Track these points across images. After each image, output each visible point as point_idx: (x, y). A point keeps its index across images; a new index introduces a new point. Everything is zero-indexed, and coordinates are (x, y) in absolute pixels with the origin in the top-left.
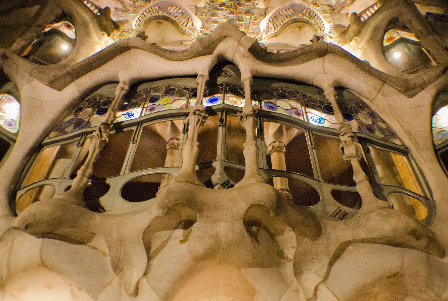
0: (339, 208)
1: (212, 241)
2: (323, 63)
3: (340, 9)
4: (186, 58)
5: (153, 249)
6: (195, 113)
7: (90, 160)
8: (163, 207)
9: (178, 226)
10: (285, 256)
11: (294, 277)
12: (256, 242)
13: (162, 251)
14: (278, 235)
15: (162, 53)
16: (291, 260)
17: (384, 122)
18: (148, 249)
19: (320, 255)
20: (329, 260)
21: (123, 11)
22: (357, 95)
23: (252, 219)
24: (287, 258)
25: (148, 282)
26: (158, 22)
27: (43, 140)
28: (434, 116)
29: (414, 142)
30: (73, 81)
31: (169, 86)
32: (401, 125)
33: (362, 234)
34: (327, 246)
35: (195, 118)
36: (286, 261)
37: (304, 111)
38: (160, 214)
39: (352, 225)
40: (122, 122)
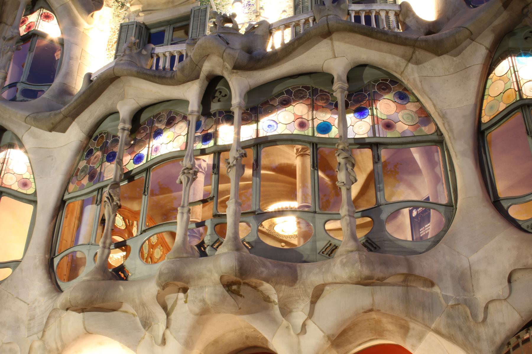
0: (330, 241)
2: (332, 44)
5: (169, 307)
6: (184, 173)
12: (239, 297)
14: (260, 286)
17: (418, 100)
18: (165, 307)
20: (310, 300)
24: (274, 302)
25: (171, 333)
27: (63, 196)
28: (491, 75)
29: (447, 128)
30: (74, 120)
32: (435, 106)
35: (185, 178)
36: (273, 304)
37: (310, 118)
39: (323, 270)
40: (132, 171)
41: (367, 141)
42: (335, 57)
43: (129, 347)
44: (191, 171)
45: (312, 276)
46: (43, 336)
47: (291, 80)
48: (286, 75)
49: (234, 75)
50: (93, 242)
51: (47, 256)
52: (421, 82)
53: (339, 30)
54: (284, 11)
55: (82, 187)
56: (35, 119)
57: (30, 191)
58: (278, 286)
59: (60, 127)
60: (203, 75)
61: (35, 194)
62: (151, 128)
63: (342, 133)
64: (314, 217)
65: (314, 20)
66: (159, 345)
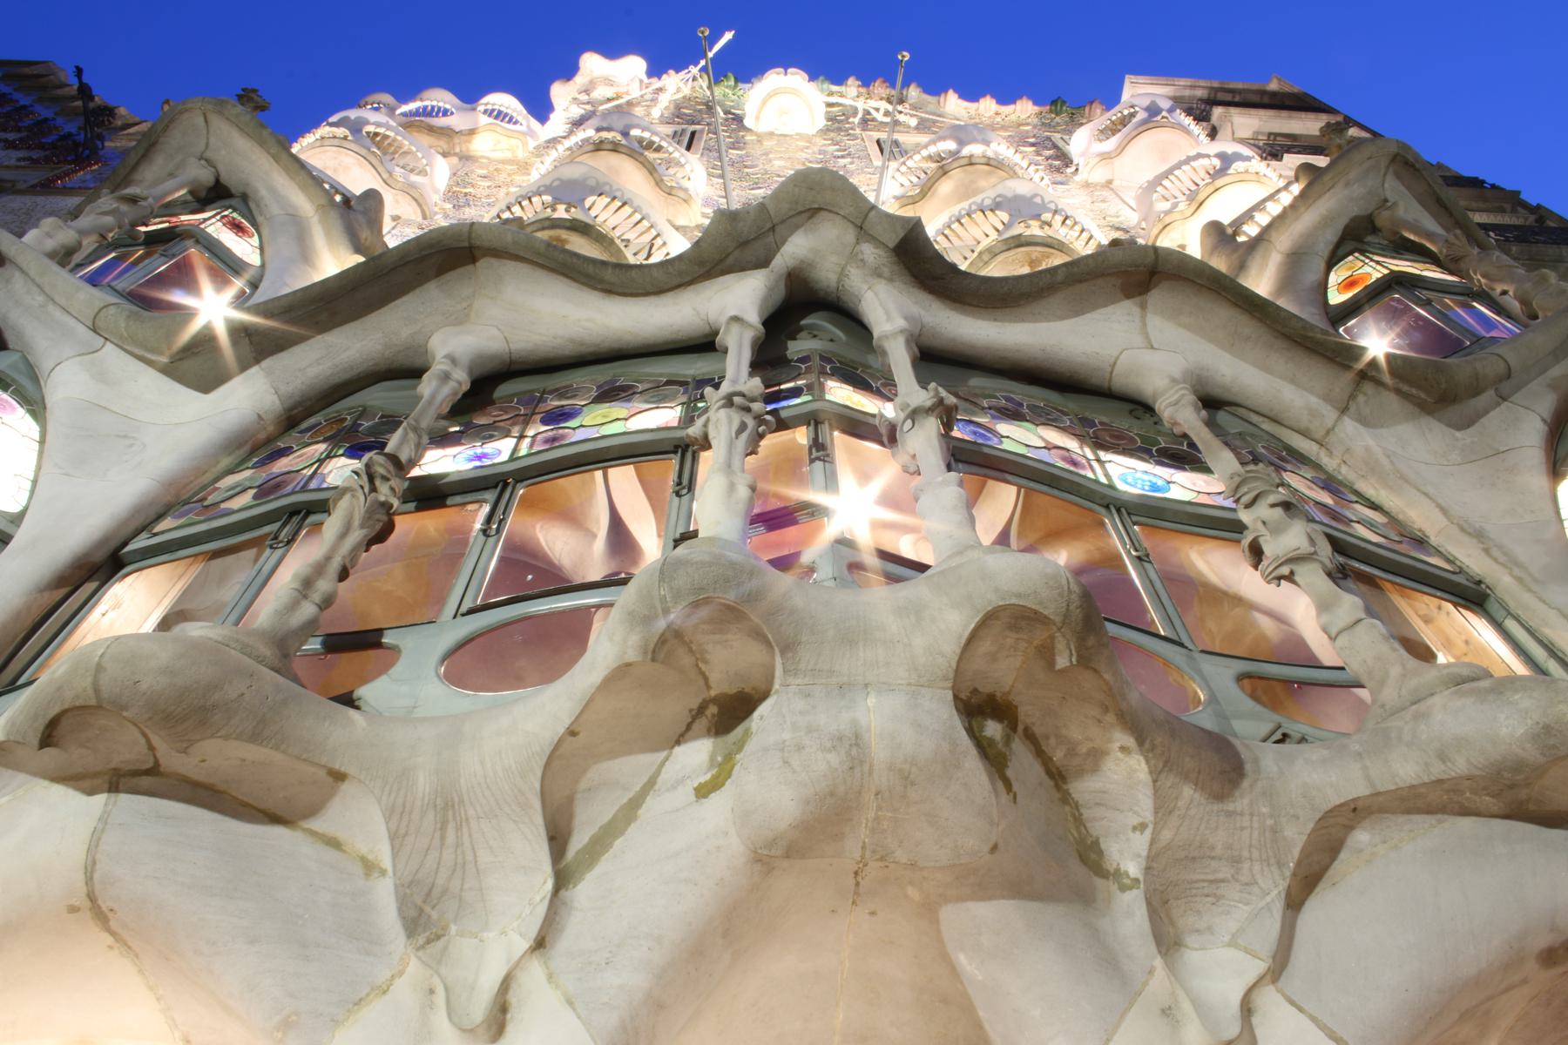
0: (1279, 727)
1: (834, 759)
2: (1143, 318)
3: (1155, 231)
4: (677, 281)
5: (578, 841)
9: (689, 727)
11: (1153, 948)
12: (1000, 784)
13: (618, 843)
14: (1081, 772)
15: (591, 269)
16: (1137, 880)
17: (1375, 507)
18: (557, 839)
19: (1246, 865)
20: (1283, 885)
22: (1267, 426)
23: (986, 688)
24: (1117, 875)
27: (125, 544)
29: (1502, 559)
30: (257, 361)
32: (1444, 511)
33: (1405, 769)
34: (1270, 822)
38: (632, 656)
58: (1168, 780)
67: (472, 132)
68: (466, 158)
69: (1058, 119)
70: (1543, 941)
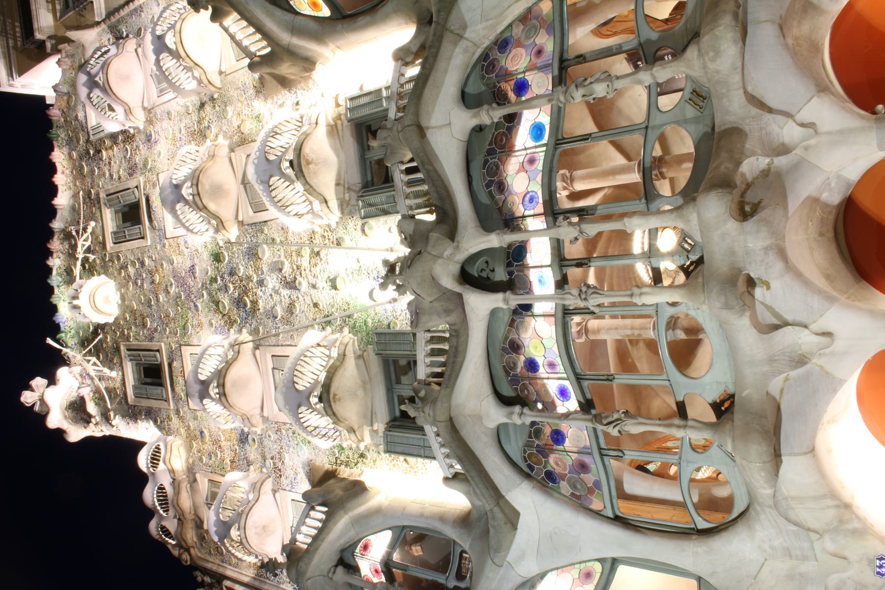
1: (771, 254)
3: (212, 88)
7: (660, 425)
8: (744, 311)
10: (767, 167)
12: (761, 205)
14: (746, 179)
17: (510, 25)
18: (776, 327)
20: (767, 114)
21: (281, 476)
22: (469, 70)
24: (769, 164)
26: (335, 402)
27: (608, 518)
30: (503, 497)
31: (503, 349)
33: (737, 78)
37: (524, 152)
39: (724, 91)
40: (579, 402)
41: (556, 72)
42: (450, 124)
43: (835, 391)
44: (584, 289)
45: (732, 108)
46: (816, 532)
47: (474, 183)
48: (467, 186)
49: (460, 245)
50: (677, 457)
51: (694, 537)
52: (487, 20)
53: (417, 114)
54: (390, 230)
55: (597, 484)
56: (497, 551)
57: (597, 568)
59: (512, 518)
60: (457, 288)
61: (601, 561)
62: (524, 378)
63: (544, 100)
64: (653, 127)
65: (402, 163)
66: (833, 340)
67: (172, 471)
68: (191, 471)
69: (63, 135)
70: (782, 38)
